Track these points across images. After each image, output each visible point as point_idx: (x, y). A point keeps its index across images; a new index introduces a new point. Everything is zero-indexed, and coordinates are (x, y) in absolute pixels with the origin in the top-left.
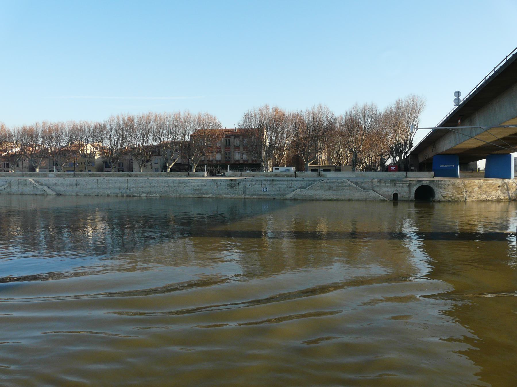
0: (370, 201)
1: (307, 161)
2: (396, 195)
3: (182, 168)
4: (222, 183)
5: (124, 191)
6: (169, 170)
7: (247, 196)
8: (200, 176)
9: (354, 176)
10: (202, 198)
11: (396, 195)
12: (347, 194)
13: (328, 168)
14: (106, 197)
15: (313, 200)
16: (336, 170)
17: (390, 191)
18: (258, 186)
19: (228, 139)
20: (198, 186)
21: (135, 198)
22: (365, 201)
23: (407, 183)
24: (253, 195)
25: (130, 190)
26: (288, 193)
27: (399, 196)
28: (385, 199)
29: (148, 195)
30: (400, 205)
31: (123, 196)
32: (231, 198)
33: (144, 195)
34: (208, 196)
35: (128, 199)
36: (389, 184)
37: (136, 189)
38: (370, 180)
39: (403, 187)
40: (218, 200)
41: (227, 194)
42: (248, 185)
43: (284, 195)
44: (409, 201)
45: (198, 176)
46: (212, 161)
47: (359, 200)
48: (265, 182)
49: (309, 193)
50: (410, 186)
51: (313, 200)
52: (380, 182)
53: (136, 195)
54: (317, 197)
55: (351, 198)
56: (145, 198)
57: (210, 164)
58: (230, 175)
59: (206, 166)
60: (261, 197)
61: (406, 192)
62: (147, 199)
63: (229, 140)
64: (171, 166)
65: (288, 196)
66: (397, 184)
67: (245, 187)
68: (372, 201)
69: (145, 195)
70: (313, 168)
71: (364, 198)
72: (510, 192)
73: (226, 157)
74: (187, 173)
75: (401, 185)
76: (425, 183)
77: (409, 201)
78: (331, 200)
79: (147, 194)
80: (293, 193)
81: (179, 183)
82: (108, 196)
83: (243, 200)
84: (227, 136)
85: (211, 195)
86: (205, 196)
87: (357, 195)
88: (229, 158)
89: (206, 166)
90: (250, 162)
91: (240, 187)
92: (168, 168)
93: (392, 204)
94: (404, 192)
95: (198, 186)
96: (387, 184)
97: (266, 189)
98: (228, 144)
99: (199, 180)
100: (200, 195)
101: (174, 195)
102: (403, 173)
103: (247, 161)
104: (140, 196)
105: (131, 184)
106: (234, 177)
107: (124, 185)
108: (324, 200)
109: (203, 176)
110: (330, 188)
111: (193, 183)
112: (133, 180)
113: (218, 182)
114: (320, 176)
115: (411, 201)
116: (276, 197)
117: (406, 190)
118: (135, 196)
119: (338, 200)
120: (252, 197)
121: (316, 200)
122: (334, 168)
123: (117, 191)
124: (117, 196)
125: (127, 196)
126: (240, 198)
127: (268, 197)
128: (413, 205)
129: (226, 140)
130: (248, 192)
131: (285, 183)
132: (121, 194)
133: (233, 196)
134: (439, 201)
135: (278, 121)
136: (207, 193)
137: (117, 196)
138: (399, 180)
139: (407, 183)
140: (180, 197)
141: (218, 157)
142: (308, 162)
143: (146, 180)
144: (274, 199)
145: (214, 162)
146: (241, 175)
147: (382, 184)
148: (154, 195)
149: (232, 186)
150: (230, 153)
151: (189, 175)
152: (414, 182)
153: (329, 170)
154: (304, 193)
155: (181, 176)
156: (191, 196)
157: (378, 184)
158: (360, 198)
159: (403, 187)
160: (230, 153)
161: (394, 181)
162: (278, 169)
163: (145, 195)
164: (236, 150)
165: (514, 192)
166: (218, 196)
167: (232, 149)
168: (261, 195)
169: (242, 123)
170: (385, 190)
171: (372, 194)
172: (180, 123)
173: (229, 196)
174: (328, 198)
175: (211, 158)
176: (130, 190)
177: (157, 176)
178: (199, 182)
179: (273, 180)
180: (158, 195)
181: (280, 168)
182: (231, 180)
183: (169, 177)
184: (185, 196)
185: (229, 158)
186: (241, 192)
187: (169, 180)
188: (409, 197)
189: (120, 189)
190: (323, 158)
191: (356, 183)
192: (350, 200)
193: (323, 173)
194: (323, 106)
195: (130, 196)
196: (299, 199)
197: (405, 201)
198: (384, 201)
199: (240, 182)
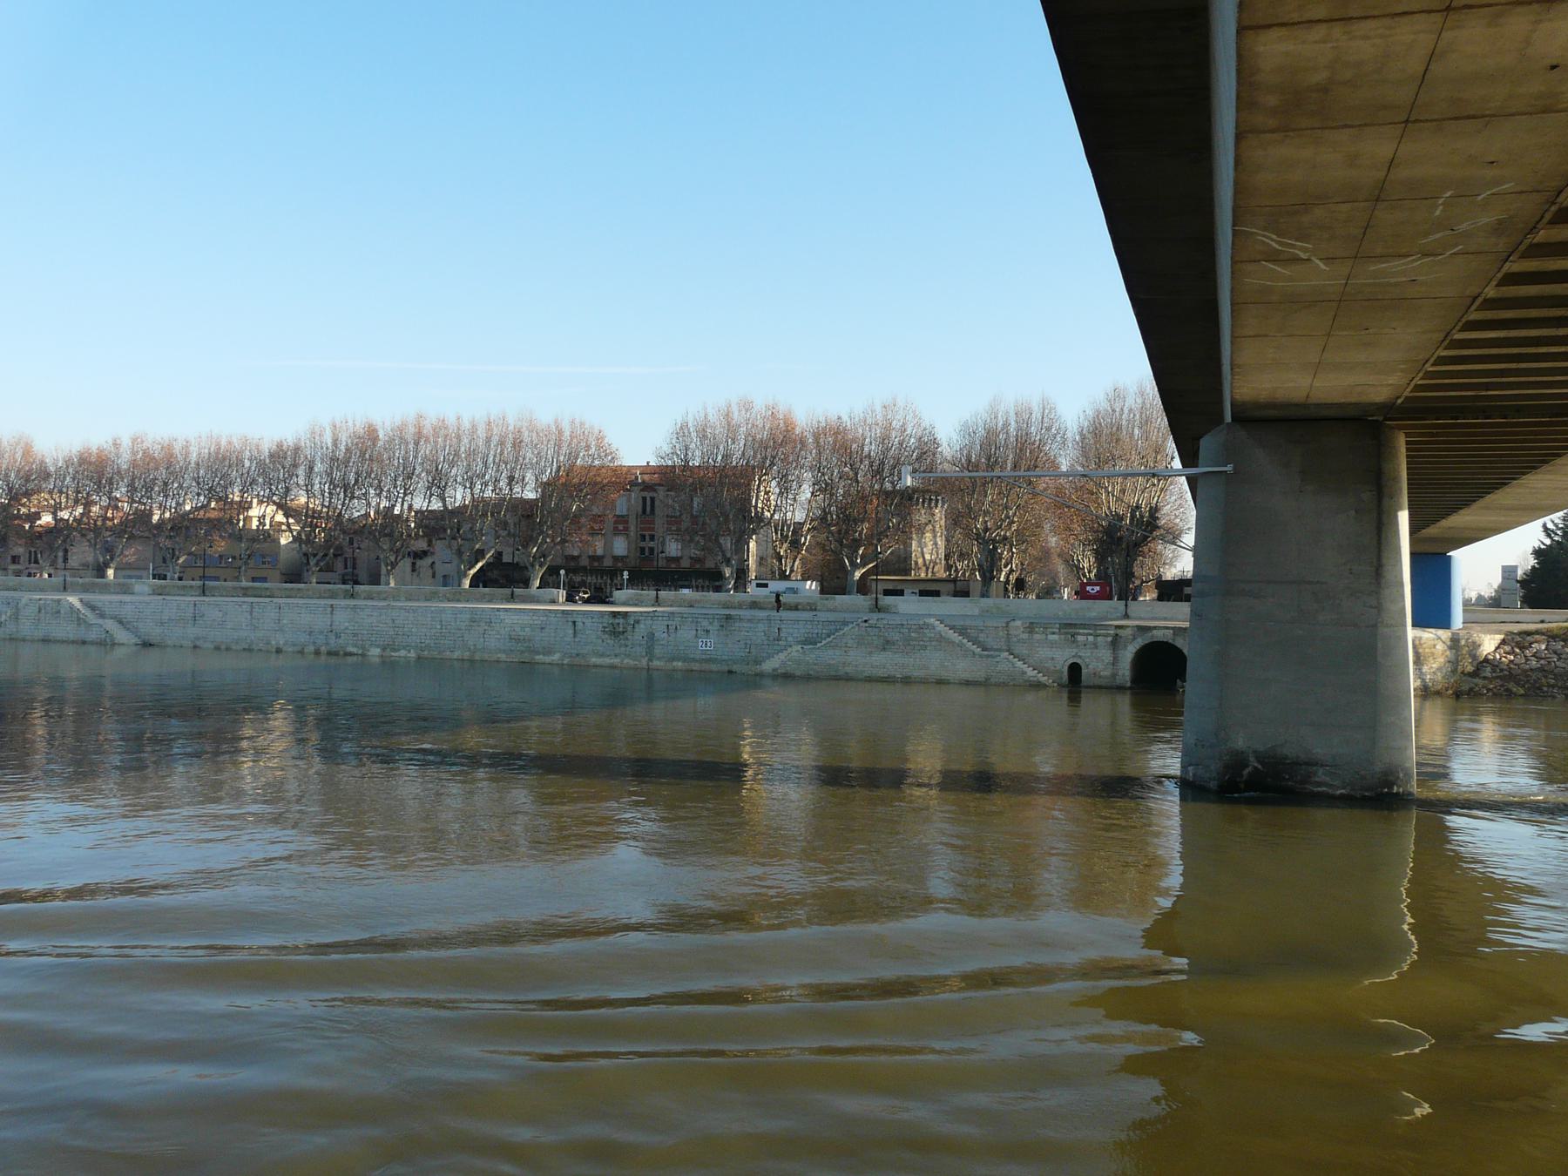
0: (998, 685)
1: (853, 564)
2: (1075, 670)
3: (503, 576)
4: (588, 622)
5: (321, 640)
6: (466, 583)
7: (656, 663)
8: (545, 602)
9: (976, 612)
10: (532, 664)
11: (1075, 670)
12: (932, 662)
13: (933, 587)
14: (274, 656)
15: (837, 678)
16: (956, 594)
17: (1060, 657)
18: (686, 634)
19: (647, 495)
20: (523, 628)
21: (350, 659)
22: (985, 684)
23: (1107, 635)
24: (674, 659)
25: (338, 636)
26: (770, 656)
27: (1084, 671)
28: (1044, 680)
29: (388, 653)
30: (1086, 698)
31: (317, 653)
32: (613, 667)
33: (375, 652)
34: (548, 659)
35: (333, 660)
36: (1056, 637)
37: (355, 635)
38: (1001, 623)
39: (1095, 646)
40: (577, 670)
41: (602, 655)
42: (659, 628)
43: (758, 662)
44: (1115, 688)
45: (538, 602)
46: (600, 559)
47: (968, 683)
48: (705, 623)
49: (827, 657)
50: (1116, 643)
51: (837, 678)
52: (1030, 628)
53: (355, 650)
54: (848, 669)
55: (944, 674)
56: (377, 660)
57: (572, 565)
58: (628, 601)
59: (562, 572)
60: (696, 666)
61: (1108, 662)
62: (383, 663)
63: (653, 499)
64: (472, 572)
65: (768, 666)
66: (1080, 638)
67: (651, 636)
68: (1004, 685)
69: (377, 651)
70: (890, 587)
71: (980, 675)
72: (1425, 669)
73: (643, 550)
74: (507, 591)
75: (1091, 638)
76: (1159, 635)
77: (1115, 688)
78: (887, 680)
79: (384, 649)
80: (782, 656)
81: (473, 620)
82: (279, 651)
83: (644, 673)
84: (647, 487)
85: (556, 657)
86: (539, 658)
87: (963, 668)
88: (652, 550)
89: (562, 572)
90: (685, 563)
91: (638, 636)
92: (465, 575)
93: (1065, 695)
94: (1098, 662)
95: (523, 628)
96: (1051, 637)
97: (707, 644)
98: (648, 509)
99: (543, 613)
100: (526, 657)
101: (456, 655)
102: (1116, 605)
103: (677, 560)
104: (363, 655)
105: (342, 619)
106: (636, 605)
107: (321, 622)
108: (870, 680)
109: (553, 602)
110: (887, 645)
111: (509, 619)
112: (347, 607)
113: (579, 620)
114: (877, 608)
115: (1120, 688)
116: (735, 668)
117: (1106, 654)
118: (351, 654)
119: (907, 681)
120: (669, 666)
121: (848, 678)
122: (951, 586)
123: (303, 638)
124: (301, 652)
125: (329, 653)
126: (636, 669)
127: (714, 667)
128: (1124, 703)
129: (644, 499)
130: (658, 651)
131: (761, 627)
132: (312, 648)
133: (616, 661)
134: (1120, 688)
135: (778, 448)
136: (549, 652)
137: (301, 652)
138: (1084, 626)
139: (1107, 635)
140: (472, 661)
141: (620, 547)
142: (855, 566)
143: (383, 608)
144: (730, 672)
145: (608, 563)
146: (657, 602)
147: (1037, 637)
148: (403, 653)
149: (615, 633)
150: (652, 538)
151: (512, 598)
152: (1129, 632)
153: (900, 593)
154: (810, 658)
155: (490, 601)
156: (503, 657)
157: (1025, 636)
158: (966, 676)
159: (1095, 646)
160: (652, 538)
161: (1070, 628)
162: (766, 586)
163: (377, 651)
164: (668, 527)
165: (1439, 669)
166: (577, 661)
167: (659, 524)
168: (694, 660)
169: (667, 449)
170: (1044, 653)
171: (1005, 664)
172: (512, 448)
173: (607, 661)
174: (881, 673)
175: (600, 552)
176: (338, 636)
177: (427, 600)
178: (526, 619)
179: (728, 617)
180: (413, 654)
181: (771, 583)
182: (615, 614)
183: (458, 601)
184: (486, 657)
185: (652, 550)
186: (638, 649)
187: (443, 610)
188: (1114, 675)
189: (311, 633)
190: (928, 557)
191: (962, 631)
192: (940, 682)
193: (889, 600)
194: (901, 403)
195: (336, 654)
196: (798, 673)
197: (1100, 687)
198: (1038, 686)
199: (638, 622)
